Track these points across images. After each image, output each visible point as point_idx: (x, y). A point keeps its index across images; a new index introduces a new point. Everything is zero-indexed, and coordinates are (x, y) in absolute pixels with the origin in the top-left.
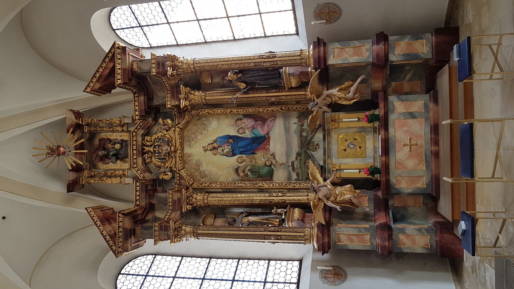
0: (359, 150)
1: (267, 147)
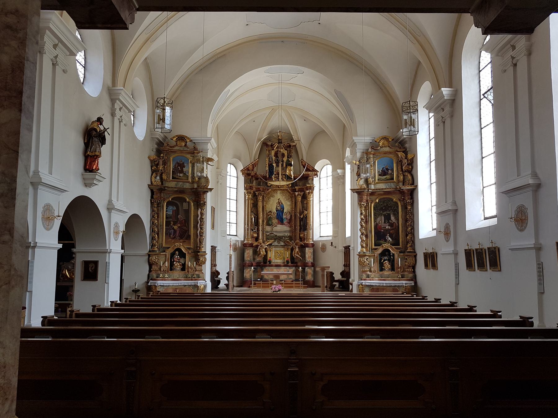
0: (277, 257)
1: (279, 224)
